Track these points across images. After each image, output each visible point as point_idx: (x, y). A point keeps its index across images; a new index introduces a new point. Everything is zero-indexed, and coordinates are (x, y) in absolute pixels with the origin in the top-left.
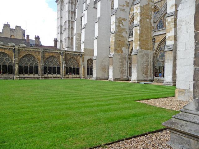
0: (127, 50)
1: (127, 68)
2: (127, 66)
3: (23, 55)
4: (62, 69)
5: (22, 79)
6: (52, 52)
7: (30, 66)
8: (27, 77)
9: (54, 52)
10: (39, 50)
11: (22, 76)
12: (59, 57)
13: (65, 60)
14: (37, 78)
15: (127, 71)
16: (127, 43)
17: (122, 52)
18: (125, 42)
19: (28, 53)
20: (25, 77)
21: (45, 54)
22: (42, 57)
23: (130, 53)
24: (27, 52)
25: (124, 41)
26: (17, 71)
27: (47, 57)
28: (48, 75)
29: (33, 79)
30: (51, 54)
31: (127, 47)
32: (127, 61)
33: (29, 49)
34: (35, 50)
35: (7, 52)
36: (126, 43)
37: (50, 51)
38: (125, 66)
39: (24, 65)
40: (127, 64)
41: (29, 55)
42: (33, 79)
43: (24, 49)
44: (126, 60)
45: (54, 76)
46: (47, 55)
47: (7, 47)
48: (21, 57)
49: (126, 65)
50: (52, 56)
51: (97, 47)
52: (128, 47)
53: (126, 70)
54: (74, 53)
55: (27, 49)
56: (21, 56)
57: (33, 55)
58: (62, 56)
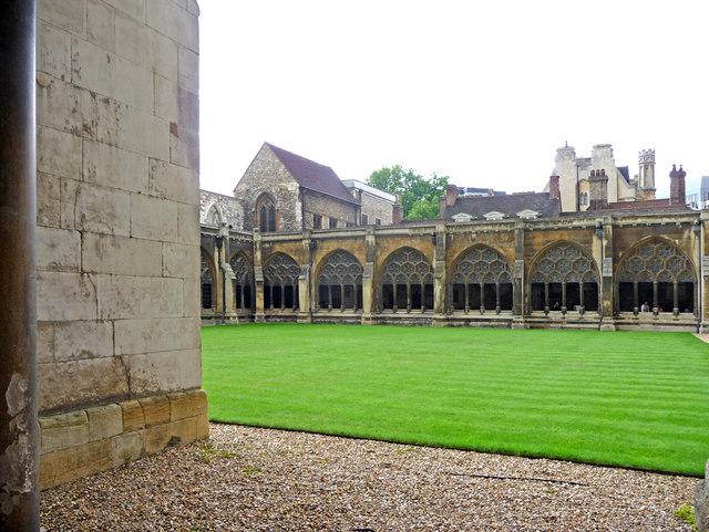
3: (460, 248)
5: (460, 326)
6: (559, 229)
8: (477, 320)
9: (567, 229)
10: (509, 229)
11: (460, 315)
12: (589, 242)
13: (611, 253)
20: (469, 320)
22: (518, 250)
27: (539, 248)
28: (547, 313)
29: (492, 326)
30: (556, 237)
33: (478, 228)
35: (417, 245)
37: (551, 226)
39: (467, 281)
41: (481, 246)
42: (492, 326)
43: (462, 231)
45: (574, 319)
46: (539, 239)
47: (417, 232)
50: (562, 243)
55: (471, 229)
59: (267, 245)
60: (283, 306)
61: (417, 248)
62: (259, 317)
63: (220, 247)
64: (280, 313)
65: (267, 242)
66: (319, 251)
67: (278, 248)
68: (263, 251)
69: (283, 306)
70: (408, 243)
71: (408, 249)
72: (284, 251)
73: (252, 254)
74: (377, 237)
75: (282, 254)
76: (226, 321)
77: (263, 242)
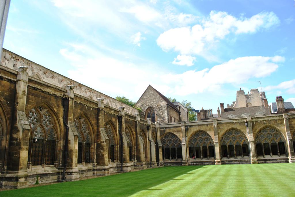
3: (259, 128)
7: (271, 143)
10: (280, 118)
11: (261, 158)
14: (284, 161)
19: (265, 125)
21: (292, 122)
24: (265, 124)
26: (253, 151)
34: (275, 118)
39: (263, 142)
41: (268, 127)
48: (257, 131)
55: (263, 119)
56: (256, 129)
57: (274, 125)
59: (162, 129)
60: (171, 158)
61: (238, 128)
62: (161, 163)
63: (148, 130)
64: (169, 161)
65: (163, 128)
66: (189, 131)
67: (168, 131)
68: (160, 131)
69: (171, 158)
70: (233, 126)
71: (233, 129)
72: (171, 131)
73: (156, 134)
74: (218, 124)
75: (170, 133)
76: (153, 166)
77: (161, 128)
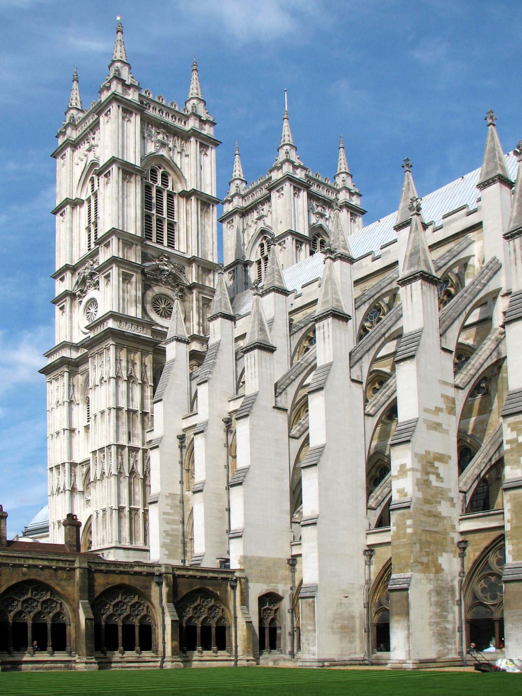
0: (457, 561)
1: (457, 625)
2: (457, 617)
4: (160, 631)
15: (458, 634)
16: (458, 538)
17: (439, 569)
18: (447, 534)
23: (467, 571)
25: (445, 533)
31: (451, 552)
32: (457, 598)
36: (452, 539)
38: (450, 617)
40: (456, 608)
44: (453, 595)
49: (454, 612)
51: (316, 555)
52: (458, 551)
53: (454, 632)
54: (205, 574)
58: (159, 584)
